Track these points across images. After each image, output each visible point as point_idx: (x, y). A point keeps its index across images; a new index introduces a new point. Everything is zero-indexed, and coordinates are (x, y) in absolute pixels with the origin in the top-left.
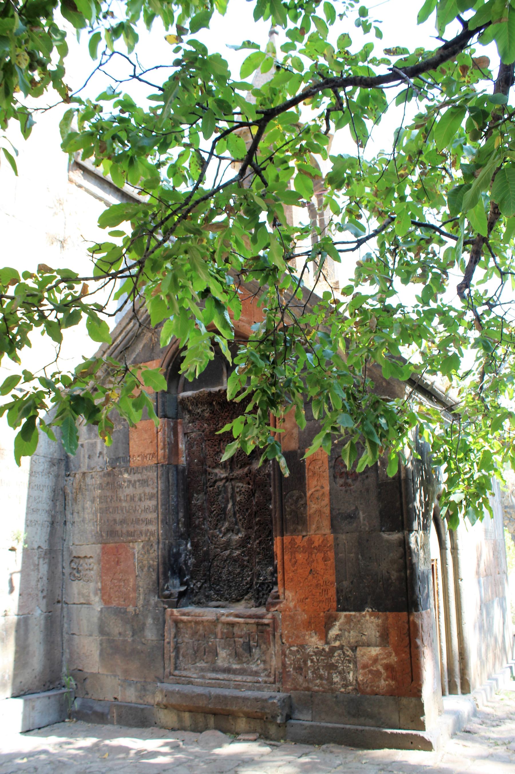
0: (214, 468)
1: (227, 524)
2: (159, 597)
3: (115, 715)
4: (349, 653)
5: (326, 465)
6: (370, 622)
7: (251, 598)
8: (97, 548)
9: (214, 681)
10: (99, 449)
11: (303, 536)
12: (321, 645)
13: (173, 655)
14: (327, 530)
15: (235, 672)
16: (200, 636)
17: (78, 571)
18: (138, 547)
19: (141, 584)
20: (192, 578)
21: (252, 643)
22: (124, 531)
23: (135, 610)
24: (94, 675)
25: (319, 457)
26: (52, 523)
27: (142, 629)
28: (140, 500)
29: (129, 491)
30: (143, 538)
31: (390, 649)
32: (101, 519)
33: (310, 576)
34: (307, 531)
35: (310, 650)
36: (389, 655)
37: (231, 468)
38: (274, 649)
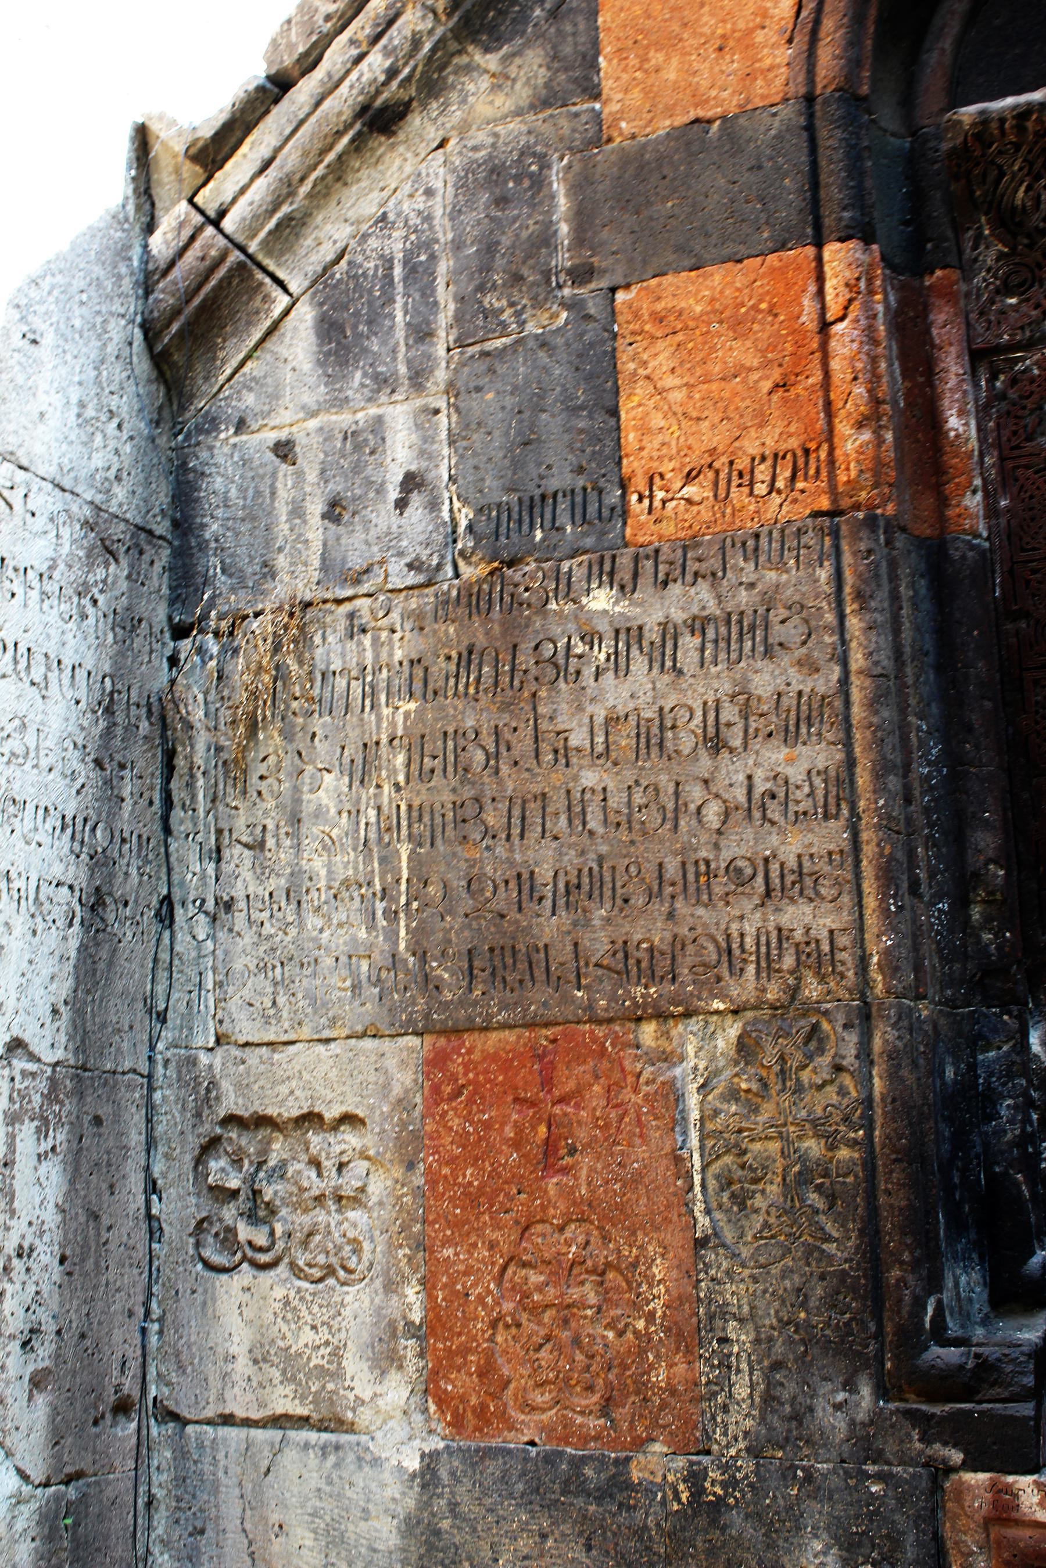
2: (882, 1391)
8: (400, 1062)
10: (400, 455)
17: (259, 1211)
18: (700, 1052)
19: (734, 1294)
22: (599, 943)
23: (695, 1478)
26: (95, 903)
29: (634, 691)
30: (745, 986)
32: (420, 878)
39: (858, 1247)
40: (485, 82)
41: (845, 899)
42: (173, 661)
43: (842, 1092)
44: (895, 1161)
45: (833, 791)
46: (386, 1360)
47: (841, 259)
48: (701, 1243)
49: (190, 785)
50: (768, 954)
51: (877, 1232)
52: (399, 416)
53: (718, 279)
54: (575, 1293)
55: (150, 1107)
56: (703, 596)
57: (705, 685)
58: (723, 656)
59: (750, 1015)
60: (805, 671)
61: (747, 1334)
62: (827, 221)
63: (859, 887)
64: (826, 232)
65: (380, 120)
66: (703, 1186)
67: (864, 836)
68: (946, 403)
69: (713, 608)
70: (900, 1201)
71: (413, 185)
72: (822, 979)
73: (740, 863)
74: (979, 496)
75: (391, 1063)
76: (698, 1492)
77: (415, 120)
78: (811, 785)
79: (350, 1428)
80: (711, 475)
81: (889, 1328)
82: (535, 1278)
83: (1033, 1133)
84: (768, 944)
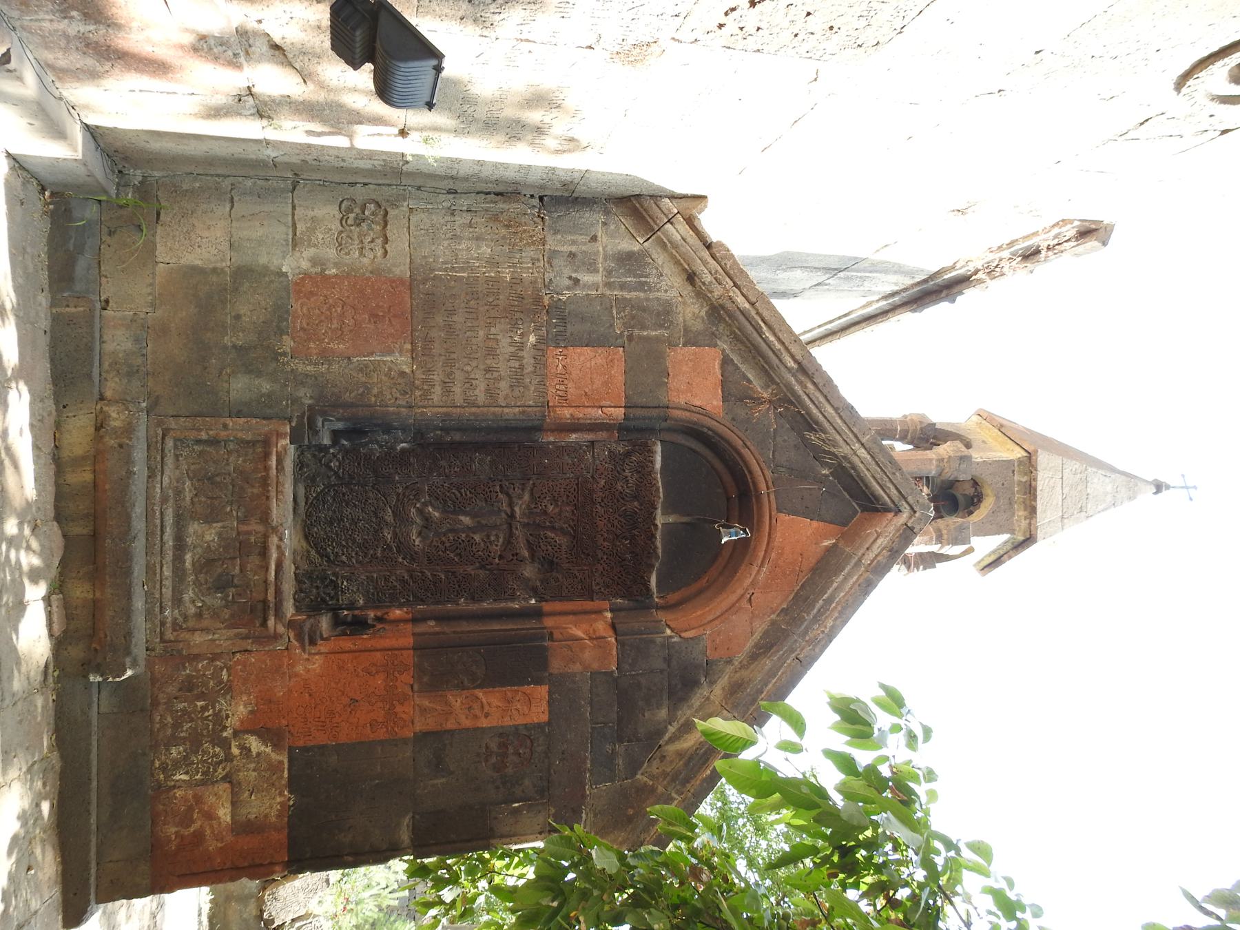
0: (532, 494)
2: (310, 406)
3: (73, 310)
4: (221, 772)
5: (520, 721)
6: (269, 804)
7: (311, 562)
8: (402, 270)
9: (158, 521)
10: (586, 278)
11: (412, 686)
12: (233, 722)
13: (204, 436)
14: (419, 727)
15: (178, 559)
16: (242, 488)
17: (359, 222)
18: (402, 361)
19: (335, 367)
20: (346, 452)
21: (231, 591)
22: (434, 334)
23: (285, 354)
24: (151, 249)
25: (533, 709)
27: (250, 369)
28: (488, 370)
29: (505, 348)
30: (420, 375)
31: (229, 838)
32: (458, 279)
33: (346, 700)
34: (420, 691)
35: (222, 704)
36: (219, 838)
37: (528, 524)
38: (223, 638)
40: (697, 311)
42: (532, 196)
46: (314, 261)
47: (619, 413)
49: (492, 202)
52: (598, 278)
53: (620, 378)
54: (335, 321)
55: (390, 185)
56: (530, 369)
57: (504, 368)
65: (691, 277)
69: (526, 371)
71: (671, 286)
75: (402, 268)
76: (281, 355)
77: (690, 288)
79: (293, 249)
82: (339, 310)
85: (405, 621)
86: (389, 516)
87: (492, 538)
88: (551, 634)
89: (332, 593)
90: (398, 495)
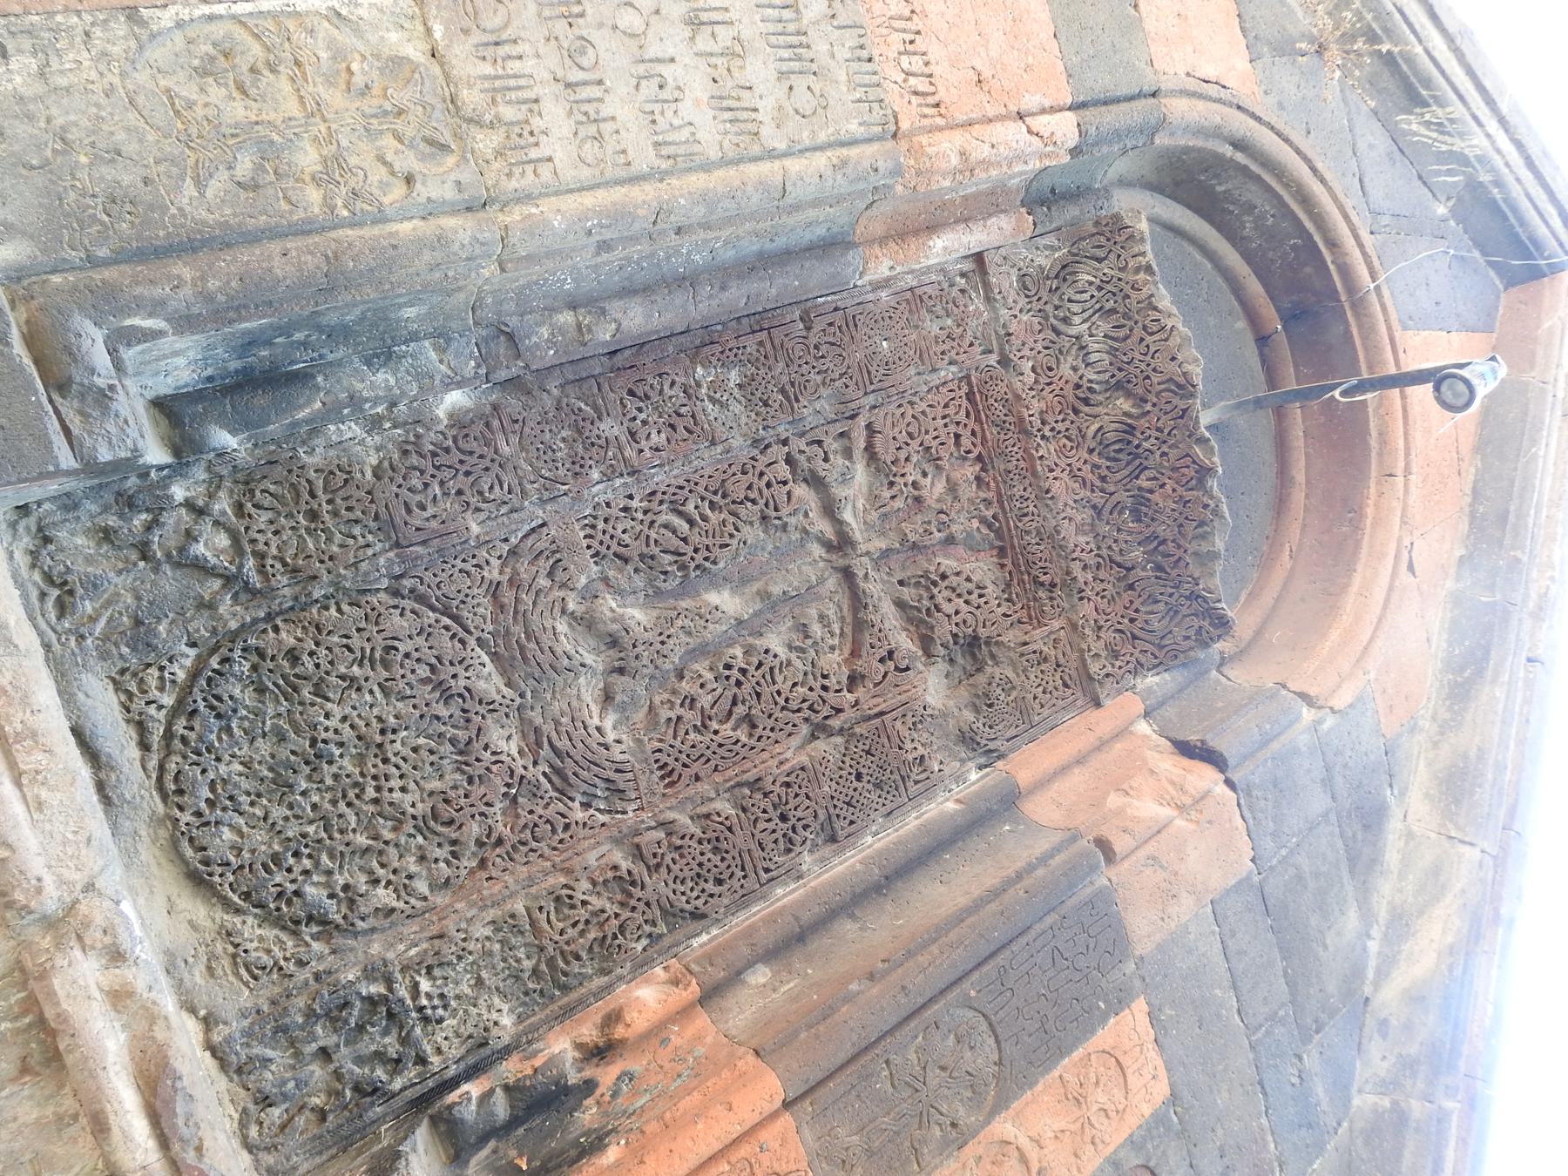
1: (637, 615)
7: (255, 971)
20: (247, 482)
37: (886, 553)
39: (204, 223)
41: (586, 173)
43: (384, 186)
44: (327, 257)
45: (681, 150)
47: (1065, 127)
48: (132, 14)
50: (509, 89)
51: (229, 246)
58: (771, 27)
59: (437, 70)
60: (776, 113)
61: (25, 84)
62: (1089, 113)
63: (597, 186)
64: (1080, 112)
66: (211, 18)
67: (647, 187)
68: (951, 236)
70: (280, 268)
72: (499, 153)
73: (590, 50)
74: (887, 273)
78: (680, 127)
80: (907, 13)
81: (109, 274)
83: (362, 410)
84: (519, 88)
85: (683, 1014)
86: (489, 681)
87: (816, 629)
88: (1103, 845)
89: (391, 1045)
90: (495, 590)
